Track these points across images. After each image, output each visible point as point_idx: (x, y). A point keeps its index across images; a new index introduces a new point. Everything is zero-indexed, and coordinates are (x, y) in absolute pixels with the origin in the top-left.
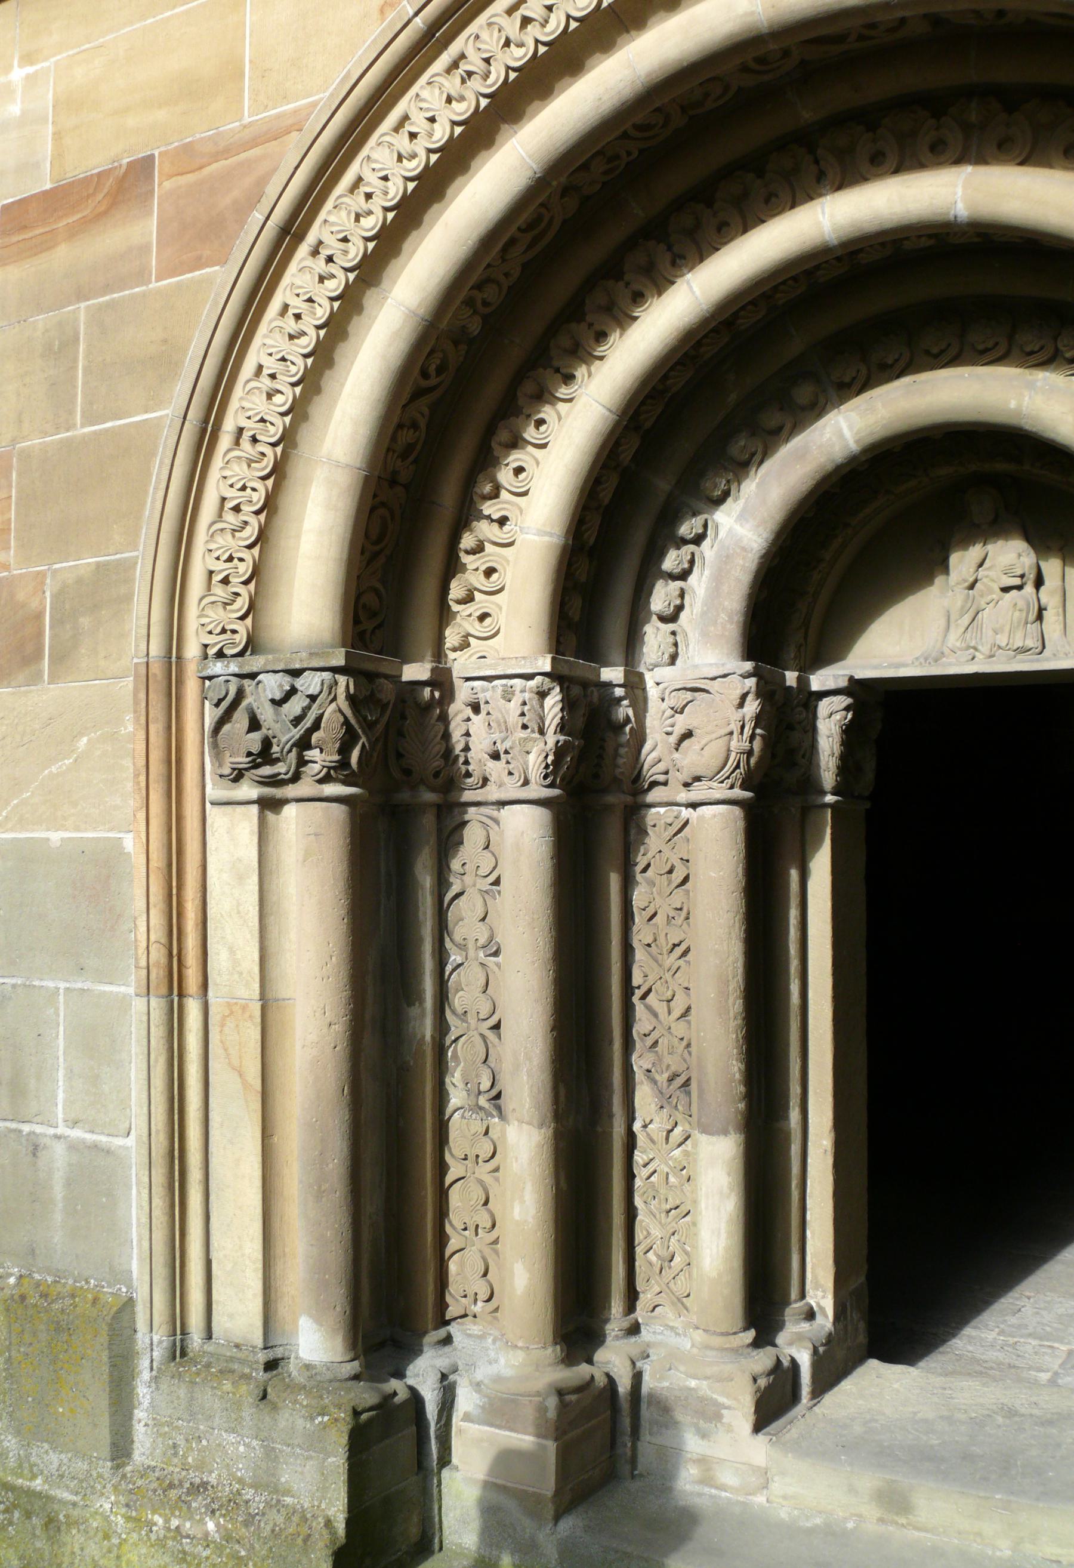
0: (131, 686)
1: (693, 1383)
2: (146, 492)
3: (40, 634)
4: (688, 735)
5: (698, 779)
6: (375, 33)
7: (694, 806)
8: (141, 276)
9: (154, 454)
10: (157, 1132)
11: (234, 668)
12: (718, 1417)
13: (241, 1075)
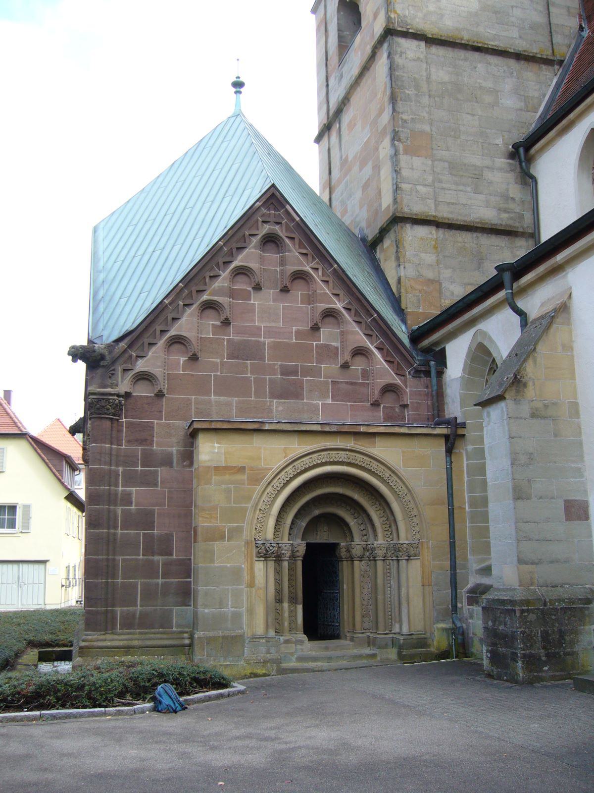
3: (225, 534)
4: (298, 551)
7: (295, 560)
8: (244, 484)
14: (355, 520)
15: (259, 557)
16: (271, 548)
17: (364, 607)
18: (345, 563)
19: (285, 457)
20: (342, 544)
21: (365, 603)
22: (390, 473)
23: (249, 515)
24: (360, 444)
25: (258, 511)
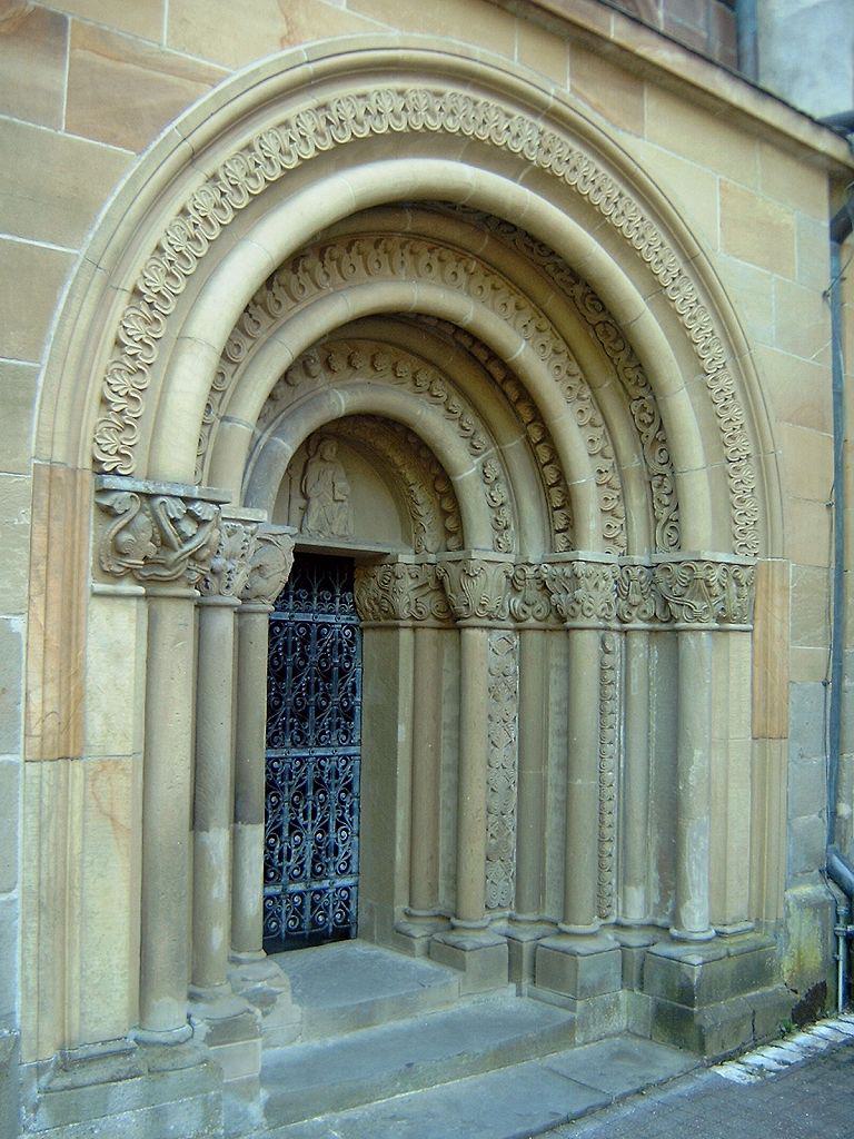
0: (29, 483)
1: (259, 985)
2: (49, 313)
5: (257, 597)
6: (274, 56)
8: (50, 117)
9: (60, 282)
10: (49, 880)
11: (140, 487)
12: (274, 1001)
13: (112, 819)
14: (476, 461)
15: (117, 577)
16: (188, 527)
17: (492, 818)
18: (405, 636)
19: (285, 41)
20: (403, 558)
21: (496, 804)
22: (680, 264)
23: (71, 312)
24: (593, 99)
25: (121, 302)
